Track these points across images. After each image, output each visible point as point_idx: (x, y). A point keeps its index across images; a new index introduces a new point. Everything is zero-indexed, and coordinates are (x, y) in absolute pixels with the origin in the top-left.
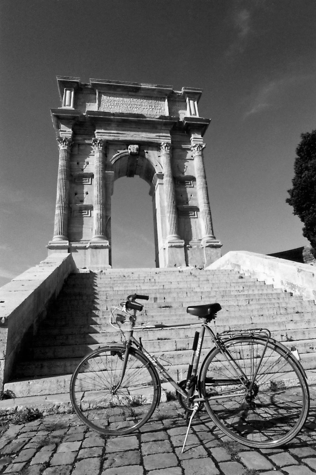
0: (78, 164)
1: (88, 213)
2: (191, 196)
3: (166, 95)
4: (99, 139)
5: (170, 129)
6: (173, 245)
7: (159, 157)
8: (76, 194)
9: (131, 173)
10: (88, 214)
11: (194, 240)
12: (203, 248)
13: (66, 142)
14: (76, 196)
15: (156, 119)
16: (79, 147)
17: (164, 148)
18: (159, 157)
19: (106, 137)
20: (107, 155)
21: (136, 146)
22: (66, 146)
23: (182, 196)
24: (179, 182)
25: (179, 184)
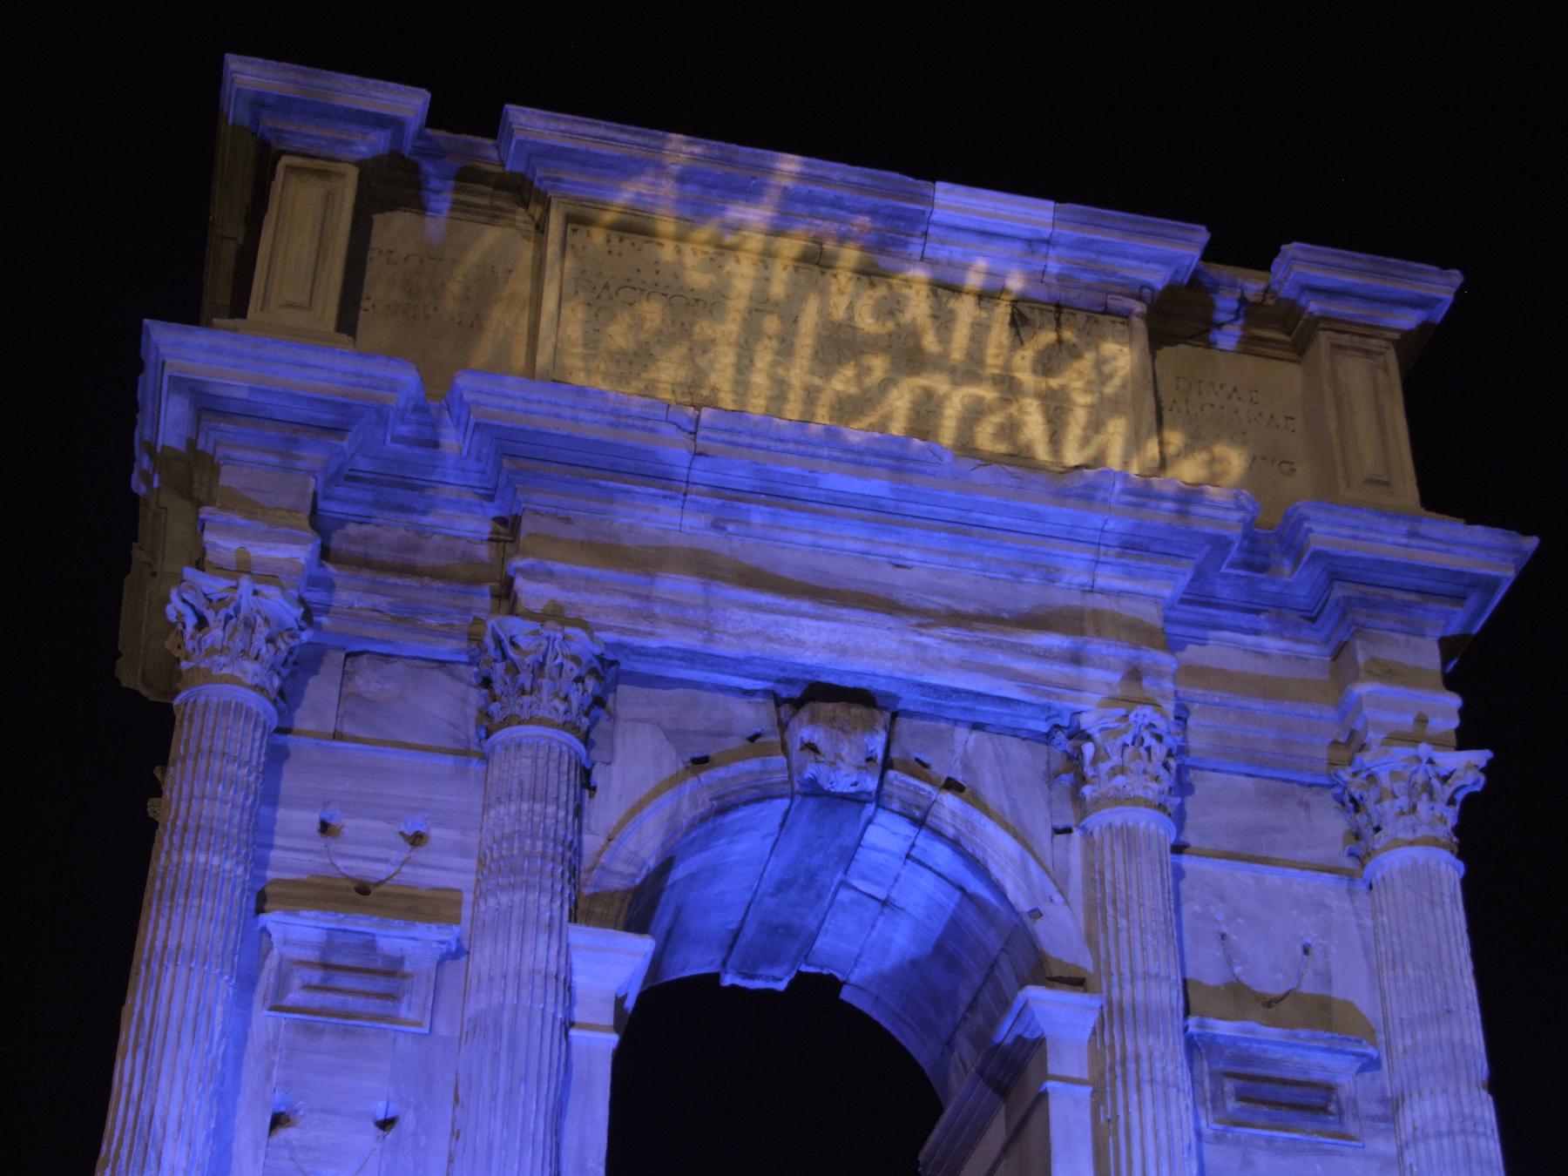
0: (325, 827)
7: (1057, 831)
13: (250, 626)
14: (283, 1133)
16: (346, 676)
18: (1057, 831)
20: (598, 778)
24: (1229, 1086)
25: (1231, 1104)
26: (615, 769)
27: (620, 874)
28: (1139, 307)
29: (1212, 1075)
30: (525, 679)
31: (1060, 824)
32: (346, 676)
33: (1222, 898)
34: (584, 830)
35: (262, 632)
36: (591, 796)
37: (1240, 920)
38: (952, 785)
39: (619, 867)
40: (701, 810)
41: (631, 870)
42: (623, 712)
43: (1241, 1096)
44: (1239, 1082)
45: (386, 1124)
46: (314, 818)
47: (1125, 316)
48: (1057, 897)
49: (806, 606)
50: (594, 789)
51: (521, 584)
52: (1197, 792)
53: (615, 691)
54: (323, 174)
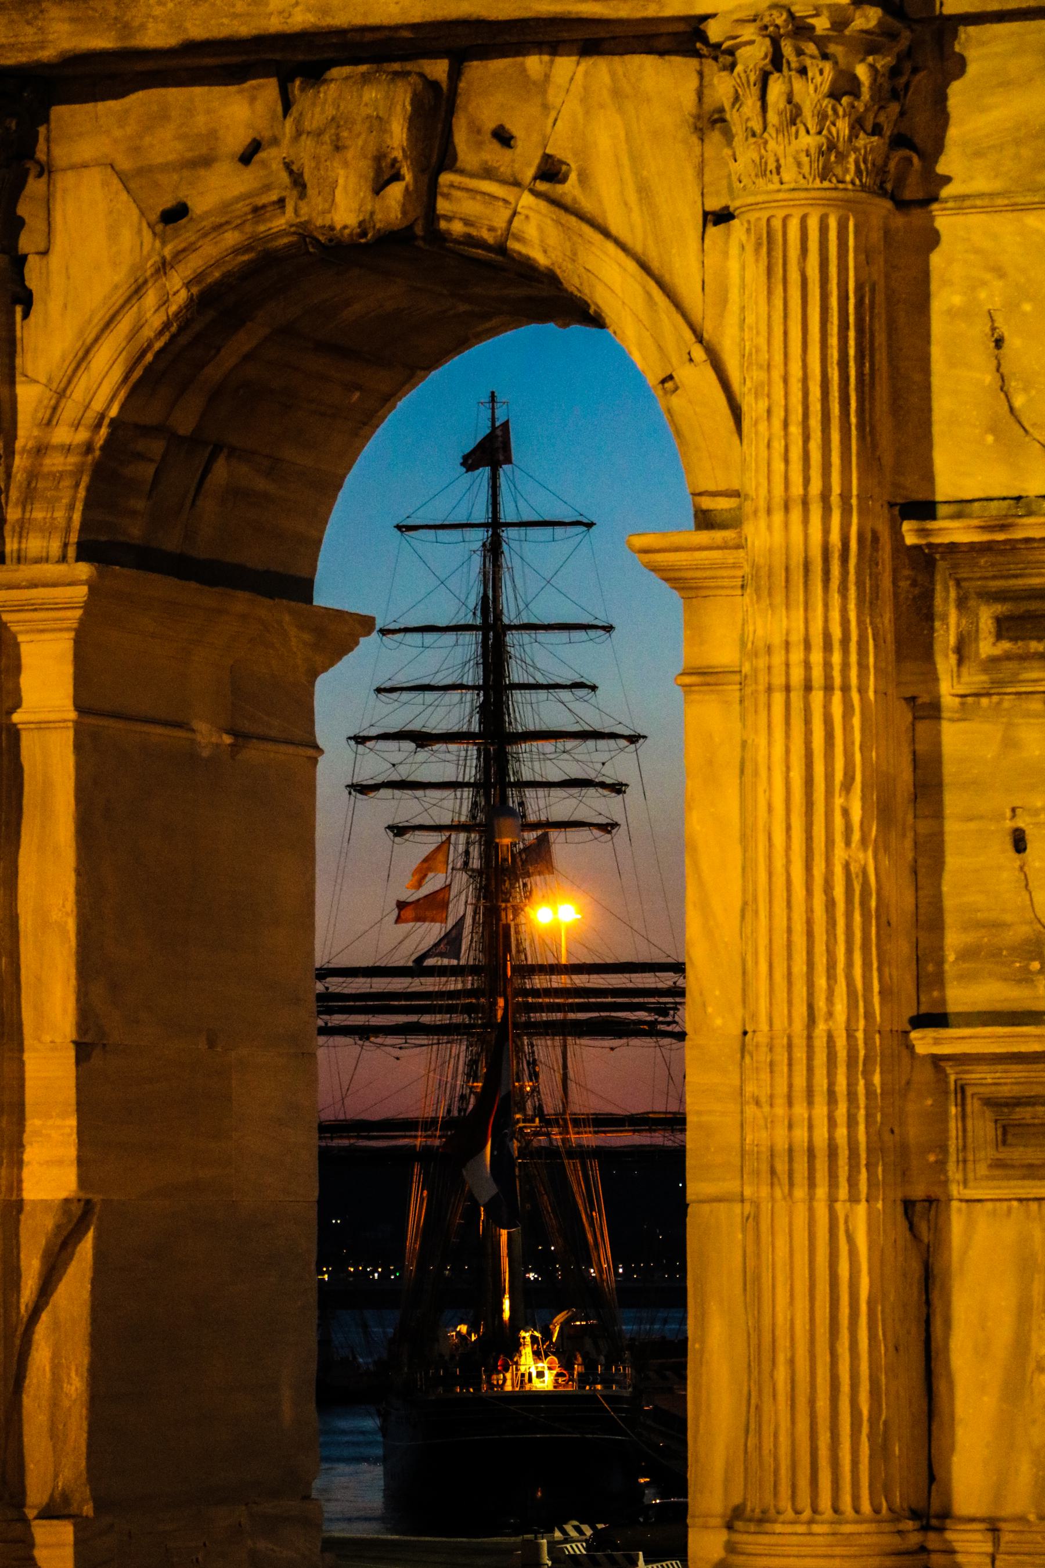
17: (751, 104)
20: (33, 279)
23: (1019, 841)
24: (986, 617)
25: (987, 647)
26: (55, 259)
27: (67, 449)
29: (962, 603)
31: (714, 204)
33: (1000, 272)
34: (19, 378)
36: (26, 315)
37: (1027, 307)
39: (62, 435)
40: (173, 308)
41: (82, 435)
42: (61, 154)
43: (1004, 628)
44: (999, 608)
48: (699, 353)
50: (26, 300)
52: (972, 69)
53: (46, 120)
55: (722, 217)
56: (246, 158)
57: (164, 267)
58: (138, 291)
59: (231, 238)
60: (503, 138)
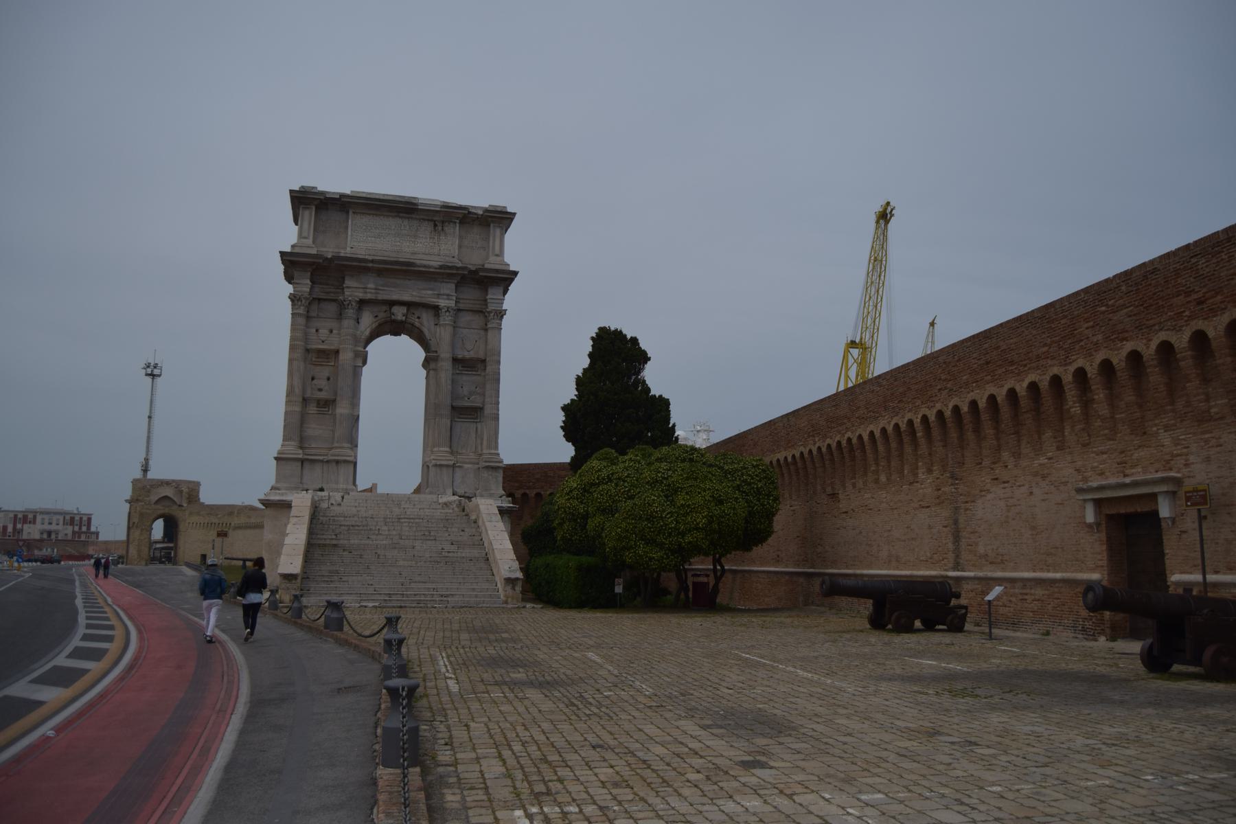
0: (317, 331)
1: (329, 409)
2: (476, 388)
3: (458, 218)
4: (350, 298)
5: (456, 281)
6: (438, 463)
8: (313, 379)
9: (396, 333)
10: (328, 411)
11: (471, 454)
12: (479, 468)
13: (301, 301)
14: (315, 382)
15: (436, 268)
16: (319, 304)
19: (360, 295)
20: (360, 321)
21: (403, 310)
22: (302, 308)
24: (460, 366)
25: (460, 368)
28: (458, 221)
30: (346, 306)
31: (436, 323)
32: (319, 304)
35: (304, 301)
38: (419, 318)
39: (363, 337)
45: (328, 379)
46: (315, 330)
47: (455, 223)
49: (393, 289)
50: (358, 323)
51: (345, 290)
54: (308, 208)
55: (437, 325)
56: (385, 311)
57: (376, 322)
58: (372, 324)
59: (383, 320)
60: (414, 314)
